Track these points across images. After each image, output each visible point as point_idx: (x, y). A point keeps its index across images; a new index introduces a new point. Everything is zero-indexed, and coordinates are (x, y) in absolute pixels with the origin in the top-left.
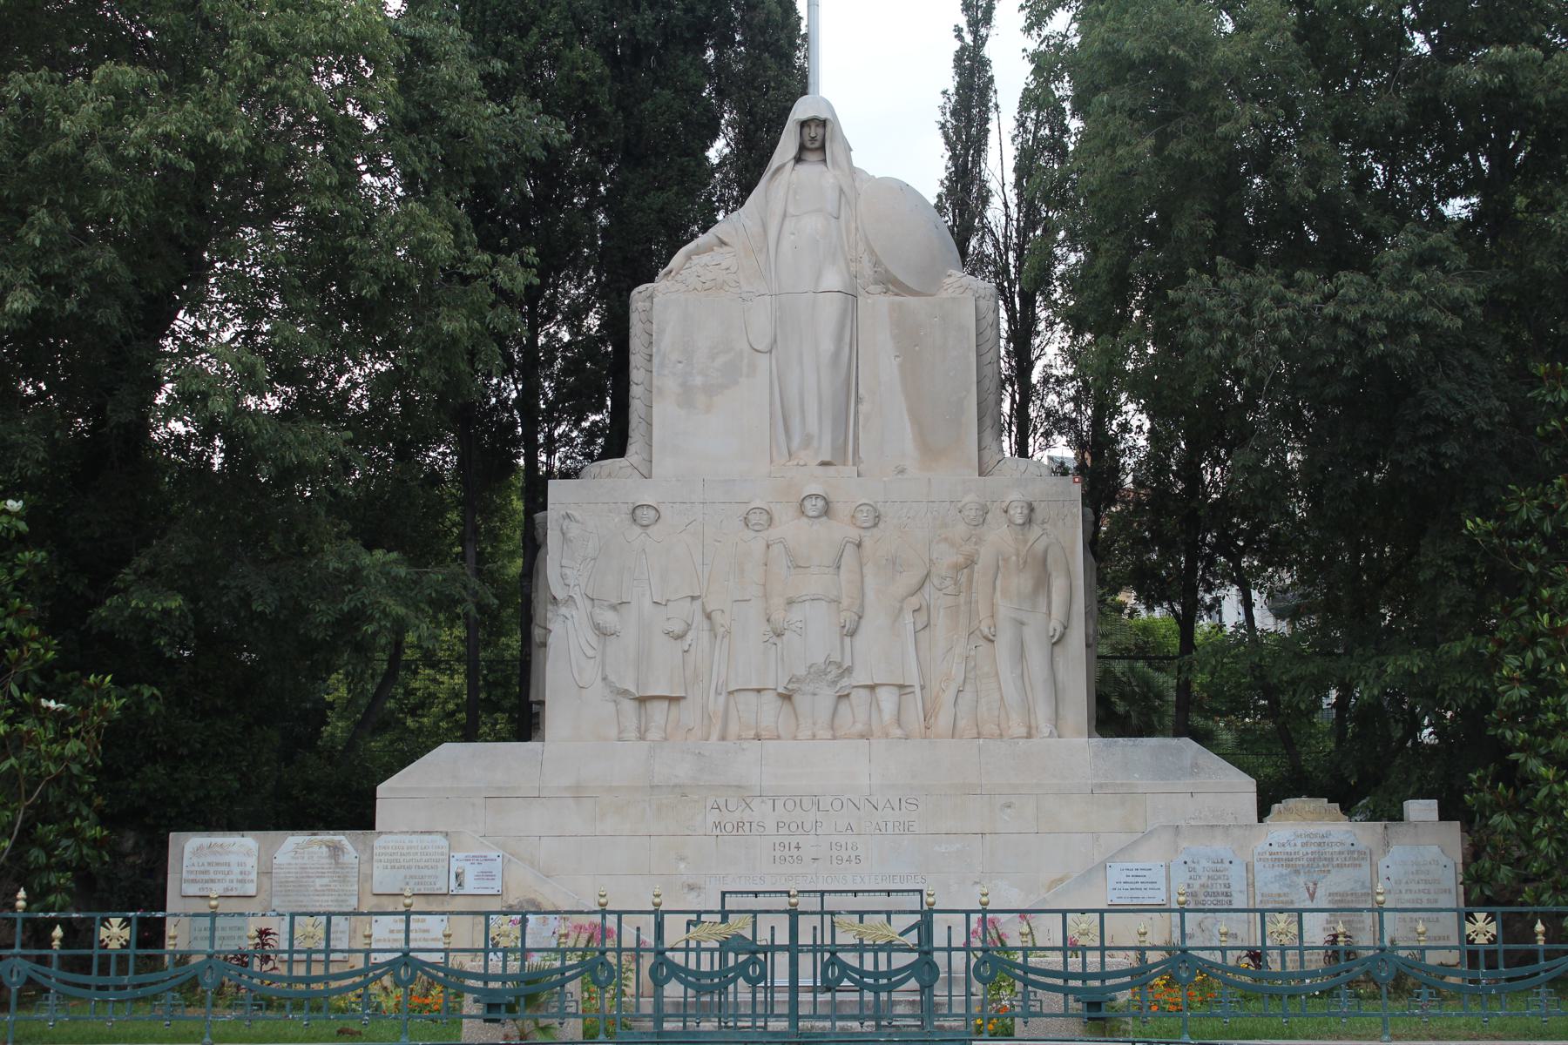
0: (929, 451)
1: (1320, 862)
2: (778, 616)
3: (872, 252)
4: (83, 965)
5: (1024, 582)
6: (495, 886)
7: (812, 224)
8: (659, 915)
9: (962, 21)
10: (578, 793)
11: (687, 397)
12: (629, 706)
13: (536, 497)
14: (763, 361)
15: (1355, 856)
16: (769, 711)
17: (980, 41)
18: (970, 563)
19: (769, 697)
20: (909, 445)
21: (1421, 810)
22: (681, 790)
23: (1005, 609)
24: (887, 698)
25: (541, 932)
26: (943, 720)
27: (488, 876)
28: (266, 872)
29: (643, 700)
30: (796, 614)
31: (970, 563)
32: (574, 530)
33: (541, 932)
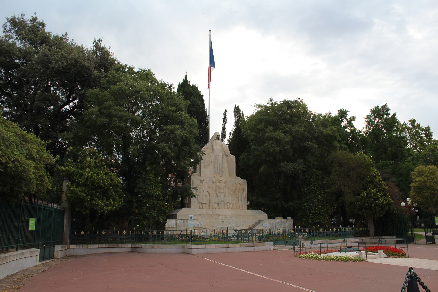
0: (230, 175)
1: (281, 224)
2: (218, 194)
3: (224, 151)
4: (100, 236)
5: (242, 191)
6: (202, 226)
7: (219, 147)
8: (274, 230)
9: (223, 123)
10: (200, 215)
11: (205, 167)
12: (201, 204)
13: (189, 179)
14: (213, 164)
15: (284, 223)
16: (216, 206)
17: (224, 126)
18: (236, 189)
19: (216, 204)
20: (228, 175)
21: (289, 218)
22: (211, 215)
23: (240, 194)
24: (228, 204)
25: (209, 232)
26: (234, 207)
27: (201, 225)
28: (176, 224)
29: (202, 204)
30: (220, 194)
31: (236, 189)
32: (194, 183)
33: (209, 232)
